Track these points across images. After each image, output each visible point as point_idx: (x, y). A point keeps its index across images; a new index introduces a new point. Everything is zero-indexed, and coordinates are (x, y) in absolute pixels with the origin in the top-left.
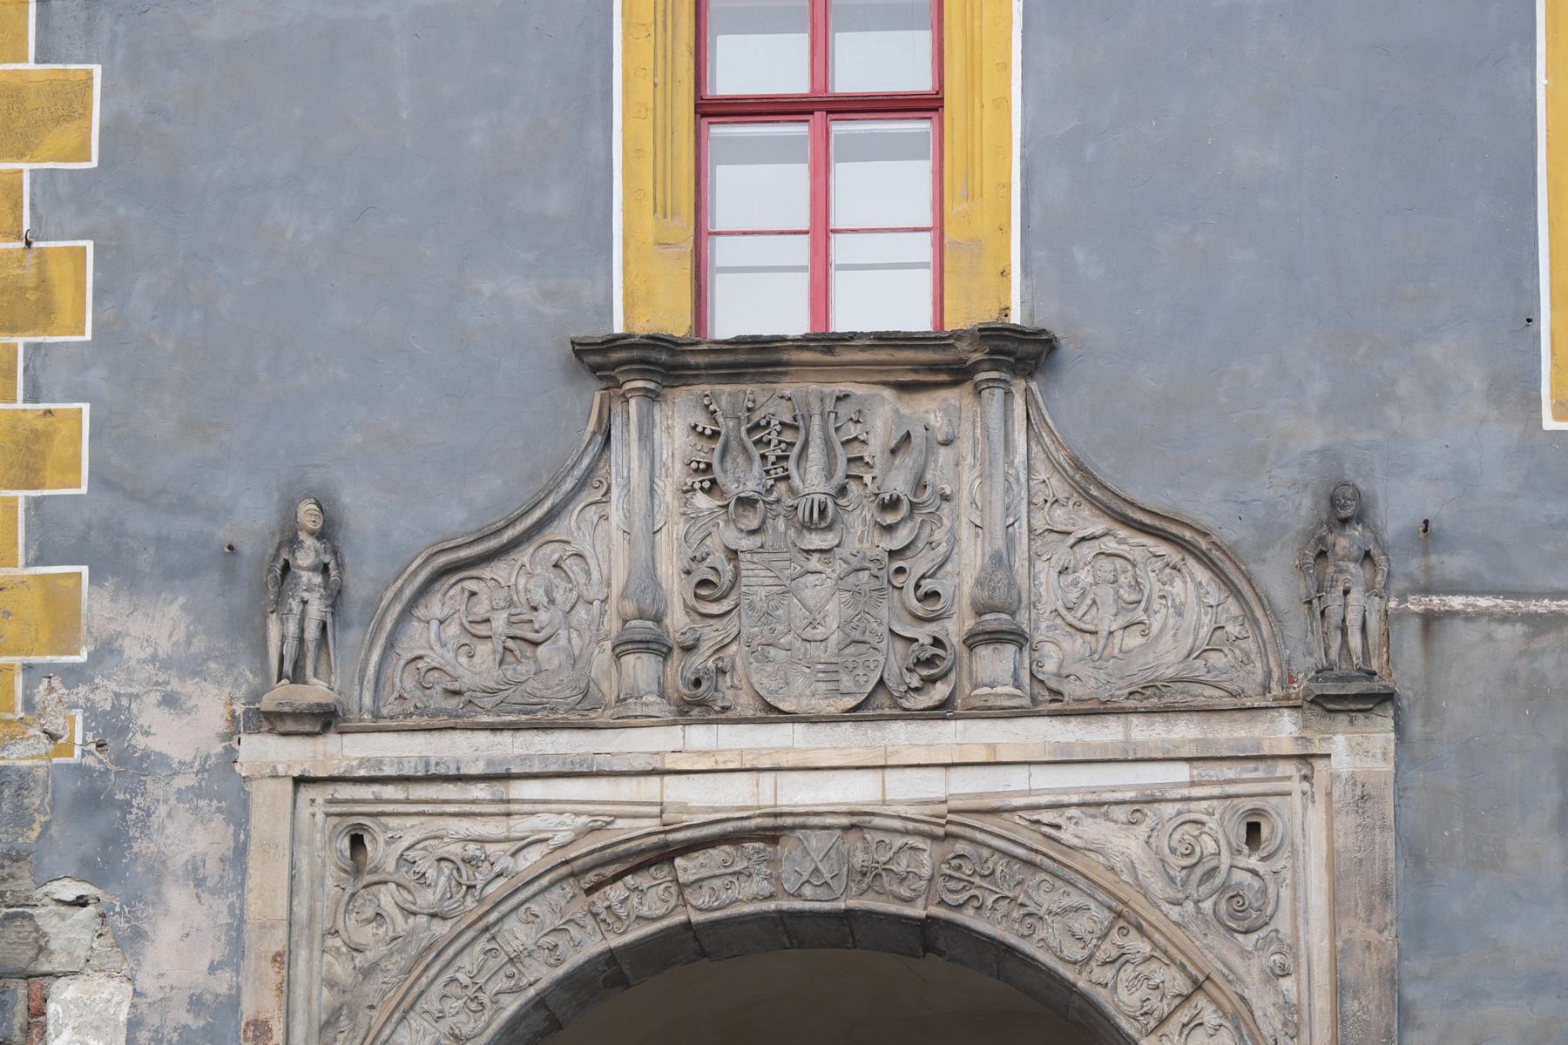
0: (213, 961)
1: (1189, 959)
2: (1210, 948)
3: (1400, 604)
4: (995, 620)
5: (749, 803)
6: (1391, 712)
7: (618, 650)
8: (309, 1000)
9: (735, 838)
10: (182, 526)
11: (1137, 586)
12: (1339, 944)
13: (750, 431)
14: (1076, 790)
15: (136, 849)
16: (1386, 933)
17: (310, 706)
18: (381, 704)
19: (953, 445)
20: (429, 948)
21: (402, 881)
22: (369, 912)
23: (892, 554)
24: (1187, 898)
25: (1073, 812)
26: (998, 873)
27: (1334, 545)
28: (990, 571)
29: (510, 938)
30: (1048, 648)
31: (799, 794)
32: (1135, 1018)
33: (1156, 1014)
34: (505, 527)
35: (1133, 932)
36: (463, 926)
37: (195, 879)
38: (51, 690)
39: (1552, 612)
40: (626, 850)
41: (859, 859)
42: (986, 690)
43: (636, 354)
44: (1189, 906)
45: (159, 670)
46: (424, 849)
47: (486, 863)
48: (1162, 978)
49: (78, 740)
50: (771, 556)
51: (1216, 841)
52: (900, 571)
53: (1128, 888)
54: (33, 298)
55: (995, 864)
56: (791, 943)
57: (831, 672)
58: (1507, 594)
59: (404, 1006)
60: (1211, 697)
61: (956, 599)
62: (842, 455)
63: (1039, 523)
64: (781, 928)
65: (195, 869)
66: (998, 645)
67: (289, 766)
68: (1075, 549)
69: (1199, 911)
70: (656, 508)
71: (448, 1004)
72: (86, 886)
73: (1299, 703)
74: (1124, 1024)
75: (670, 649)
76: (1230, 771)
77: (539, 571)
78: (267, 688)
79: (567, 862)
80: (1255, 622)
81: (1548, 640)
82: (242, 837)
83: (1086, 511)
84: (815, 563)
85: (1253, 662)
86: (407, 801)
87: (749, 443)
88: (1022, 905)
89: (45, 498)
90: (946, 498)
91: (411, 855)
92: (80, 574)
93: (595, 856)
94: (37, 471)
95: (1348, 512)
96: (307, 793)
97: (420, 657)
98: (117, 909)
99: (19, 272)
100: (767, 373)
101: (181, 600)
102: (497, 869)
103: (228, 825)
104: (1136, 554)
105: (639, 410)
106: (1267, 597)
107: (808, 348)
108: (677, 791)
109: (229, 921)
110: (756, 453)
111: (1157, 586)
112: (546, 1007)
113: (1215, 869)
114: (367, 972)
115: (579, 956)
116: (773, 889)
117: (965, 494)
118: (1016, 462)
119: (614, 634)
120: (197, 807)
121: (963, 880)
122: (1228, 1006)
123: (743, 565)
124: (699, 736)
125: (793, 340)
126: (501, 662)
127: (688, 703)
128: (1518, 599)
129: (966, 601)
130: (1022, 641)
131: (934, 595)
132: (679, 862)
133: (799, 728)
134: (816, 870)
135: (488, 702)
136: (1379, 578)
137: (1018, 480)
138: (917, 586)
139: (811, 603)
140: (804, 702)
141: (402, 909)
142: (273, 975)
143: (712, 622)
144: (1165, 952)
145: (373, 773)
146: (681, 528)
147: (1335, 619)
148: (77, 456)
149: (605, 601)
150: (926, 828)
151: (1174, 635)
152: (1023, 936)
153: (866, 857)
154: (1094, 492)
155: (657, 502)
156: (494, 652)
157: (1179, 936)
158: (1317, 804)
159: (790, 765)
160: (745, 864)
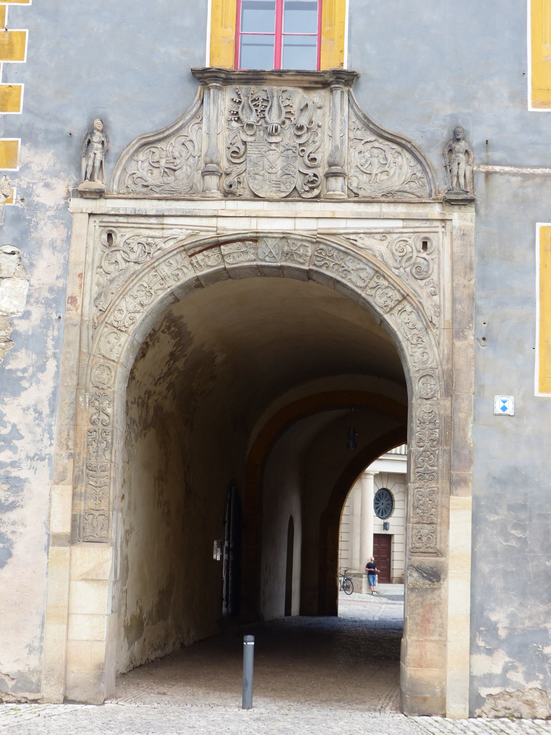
0: (57, 276)
1: (402, 288)
2: (409, 284)
5: (248, 228)
6: (474, 206)
7: (203, 174)
8: (91, 290)
9: (242, 240)
10: (54, 126)
11: (386, 159)
12: (454, 285)
13: (252, 101)
14: (363, 228)
15: (33, 235)
16: (471, 282)
17: (95, 189)
18: (120, 189)
19: (323, 109)
20: (133, 274)
21: (125, 250)
22: (113, 261)
23: (300, 145)
24: (401, 267)
25: (361, 235)
26: (334, 255)
28: (334, 152)
29: (162, 271)
30: (354, 178)
31: (264, 226)
32: (382, 307)
33: (390, 306)
34: (166, 131)
35: (382, 278)
36: (146, 267)
37: (52, 247)
38: (6, 180)
39: (531, 173)
40: (204, 243)
41: (286, 249)
42: (332, 193)
43: (213, 74)
44: (402, 270)
45: (44, 175)
47: (155, 245)
48: (392, 294)
50: (258, 144)
51: (412, 247)
52: (303, 151)
53: (380, 262)
54: (7, 48)
55: (334, 252)
56: (261, 275)
57: (278, 183)
58: (516, 166)
59: (124, 293)
61: (322, 161)
62: (284, 111)
63: (352, 136)
65: (53, 243)
66: (336, 177)
67: (87, 209)
68: (364, 145)
69: (405, 271)
70: (218, 126)
71: (139, 293)
72: (15, 248)
73: (441, 201)
74: (378, 309)
75: (222, 174)
76: (417, 224)
77: (177, 145)
78: (80, 182)
79: (183, 246)
80: (426, 173)
81: (529, 183)
82: (70, 233)
83: (368, 132)
84: (273, 147)
85: (425, 186)
86: (128, 223)
87: (252, 105)
88: (343, 267)
89: (7, 115)
90: (319, 126)
91: (128, 241)
92: (18, 141)
93: (193, 244)
94: (5, 106)
95: (460, 137)
96: (93, 219)
97: (135, 174)
98: (25, 256)
99: (3, 39)
100: (259, 82)
101: (52, 151)
102: (158, 247)
103: (65, 229)
104: (385, 148)
105: (214, 92)
106: (431, 164)
107: (273, 75)
108: (222, 223)
109: (64, 262)
110: (254, 109)
111: (393, 159)
112: (174, 294)
113: (411, 257)
114: (111, 281)
115: (186, 278)
116: (255, 258)
117: (326, 125)
118: (344, 115)
119: (202, 168)
120: (54, 222)
121: (322, 257)
122: (415, 305)
123: (248, 147)
124: (231, 205)
125: (268, 72)
126: (163, 176)
127: (227, 193)
128: (519, 168)
129: (326, 162)
130: (345, 176)
131: (314, 159)
132: (222, 247)
133: (266, 203)
134: (271, 252)
135: (157, 190)
136: (470, 159)
137: (345, 121)
138: (309, 156)
139: (271, 160)
140: (268, 194)
141: (125, 260)
142: (78, 281)
143: (236, 165)
144: (393, 285)
145: (116, 213)
146: (227, 133)
147: (455, 173)
148: (19, 101)
149: (199, 157)
150: (309, 239)
151: (398, 176)
152: (343, 277)
153: (288, 248)
154: (371, 126)
155: (219, 124)
156: (160, 172)
157: (397, 280)
158: (447, 237)
159: (262, 216)
160: (246, 249)
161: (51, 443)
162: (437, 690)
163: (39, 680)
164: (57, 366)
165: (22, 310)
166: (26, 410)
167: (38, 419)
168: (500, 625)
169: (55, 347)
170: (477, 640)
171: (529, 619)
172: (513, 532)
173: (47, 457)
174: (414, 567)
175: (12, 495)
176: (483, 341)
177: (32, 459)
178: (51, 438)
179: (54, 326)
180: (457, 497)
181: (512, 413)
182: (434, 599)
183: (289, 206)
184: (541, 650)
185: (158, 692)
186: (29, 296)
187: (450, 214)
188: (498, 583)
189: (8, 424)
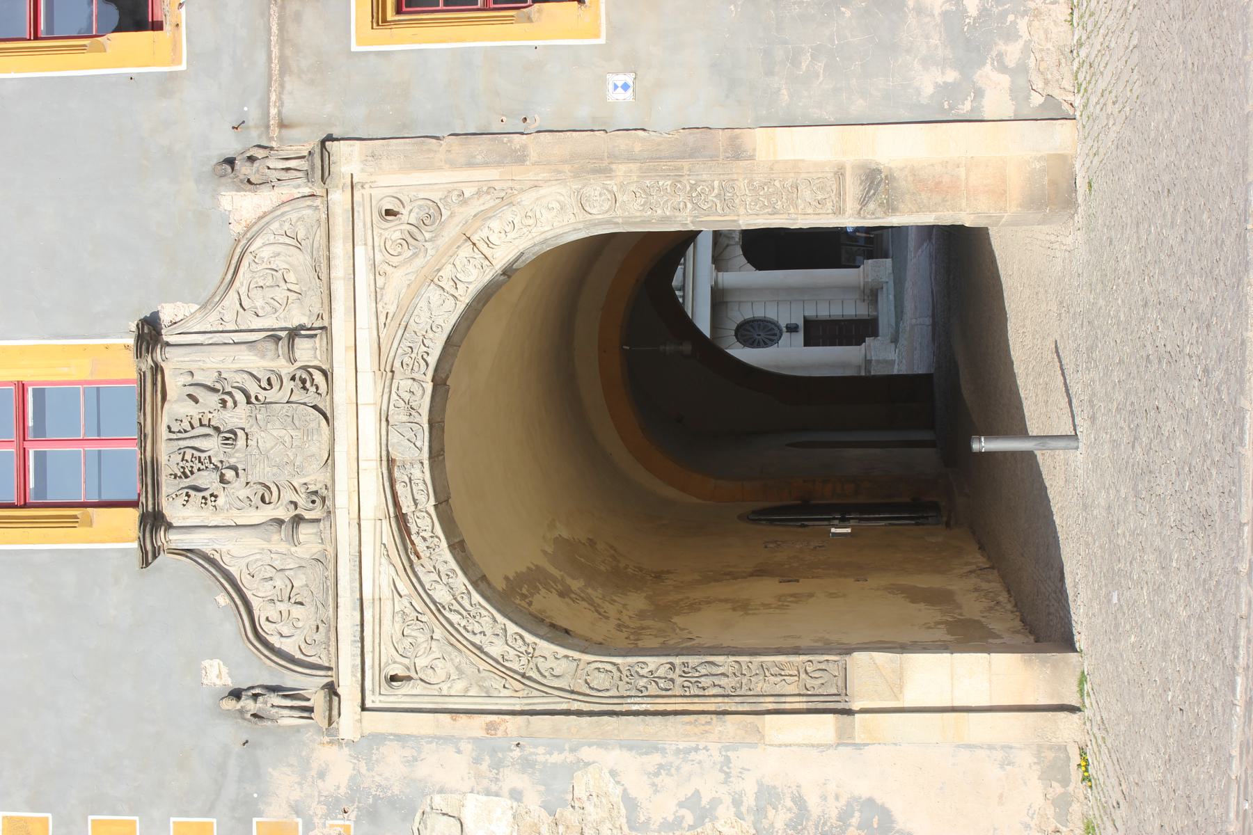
3: (274, 140)
4: (282, 348)
5: (375, 474)
7: (297, 543)
9: (392, 483)
15: (397, 792)
23: (249, 402)
25: (380, 308)
27: (245, 175)
31: (370, 450)
42: (318, 352)
46: (397, 643)
49: (341, 822)
51: (394, 231)
60: (320, 237)
64: (436, 459)
65: (408, 761)
69: (430, 240)
79: (405, 569)
83: (226, 302)
86: (373, 651)
92: (257, 822)
101: (270, 770)
103: (386, 745)
119: (288, 546)
120: (376, 761)
138: (265, 389)
139: (273, 443)
145: (360, 670)
151: (289, 256)
159: (356, 453)
161: (704, 748)
162: (1038, 167)
163: (1051, 748)
164: (590, 745)
165: (509, 802)
166: (656, 789)
167: (669, 770)
168: (940, 80)
169: (561, 751)
170: (962, 112)
171: (929, 39)
172: (804, 66)
173: (724, 753)
174: (861, 209)
175: (782, 802)
176: (528, 121)
177: (728, 775)
178: (696, 749)
179: (531, 754)
180: (757, 150)
181: (633, 75)
182: (906, 176)
183: (340, 414)
184: (972, 19)
185: (1060, 581)
186: (488, 793)
187: (343, 177)
189: (677, 814)
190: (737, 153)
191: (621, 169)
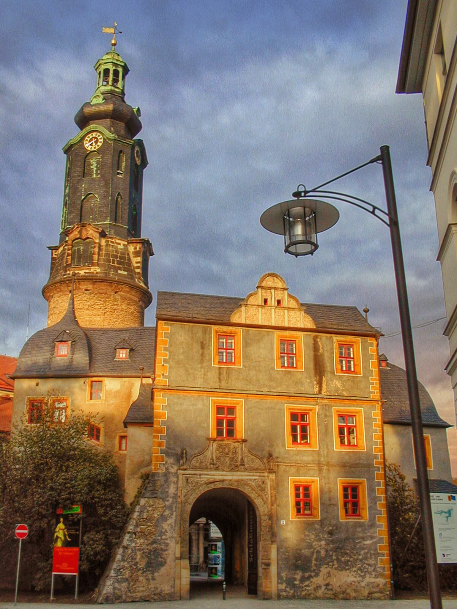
9: (220, 481)
10: (174, 451)
31: (226, 478)
108: (215, 477)
114: (188, 491)
124: (217, 472)
166: (168, 525)
188: (283, 566)
190: (273, 542)
191: (270, 522)
